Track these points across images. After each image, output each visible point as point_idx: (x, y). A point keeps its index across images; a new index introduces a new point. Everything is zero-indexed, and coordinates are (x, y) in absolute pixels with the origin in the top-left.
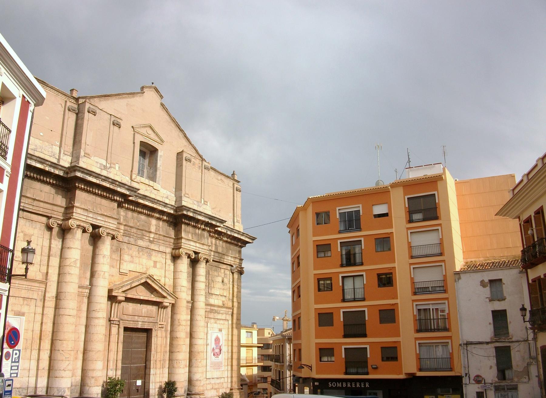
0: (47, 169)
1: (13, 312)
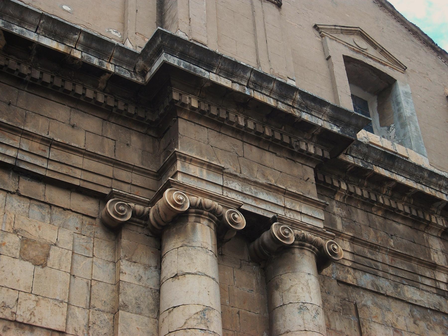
0: (77, 54)
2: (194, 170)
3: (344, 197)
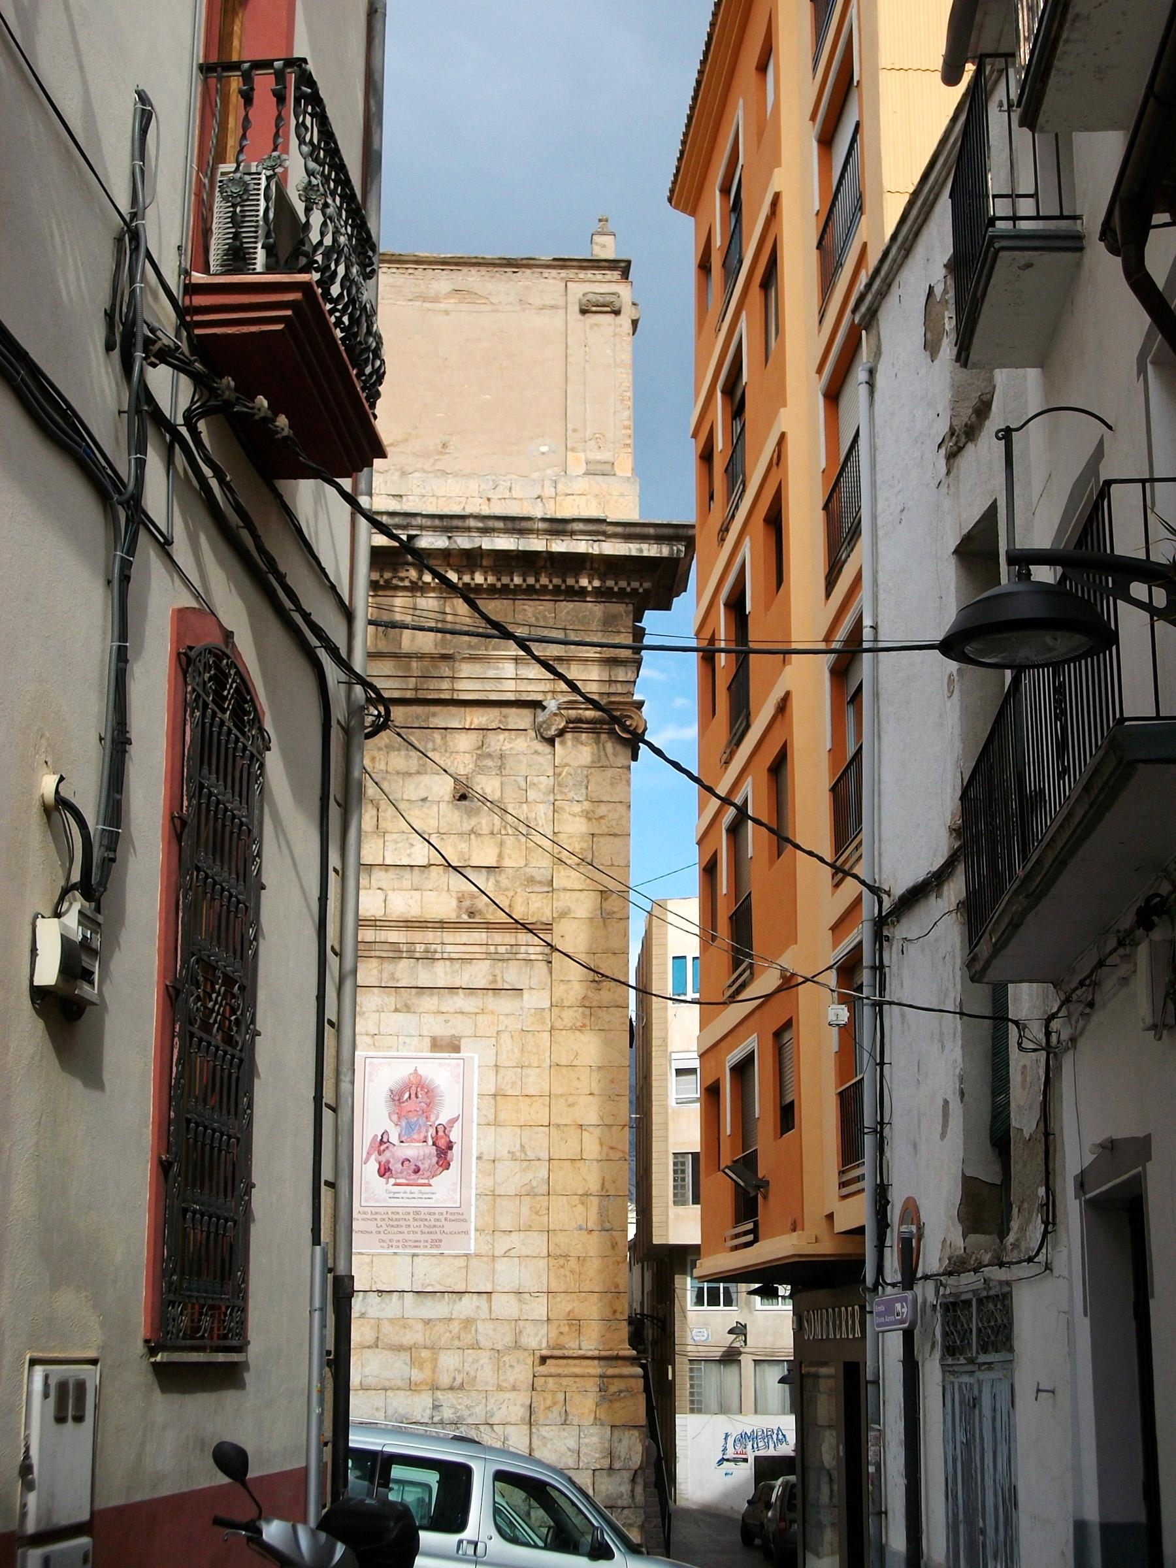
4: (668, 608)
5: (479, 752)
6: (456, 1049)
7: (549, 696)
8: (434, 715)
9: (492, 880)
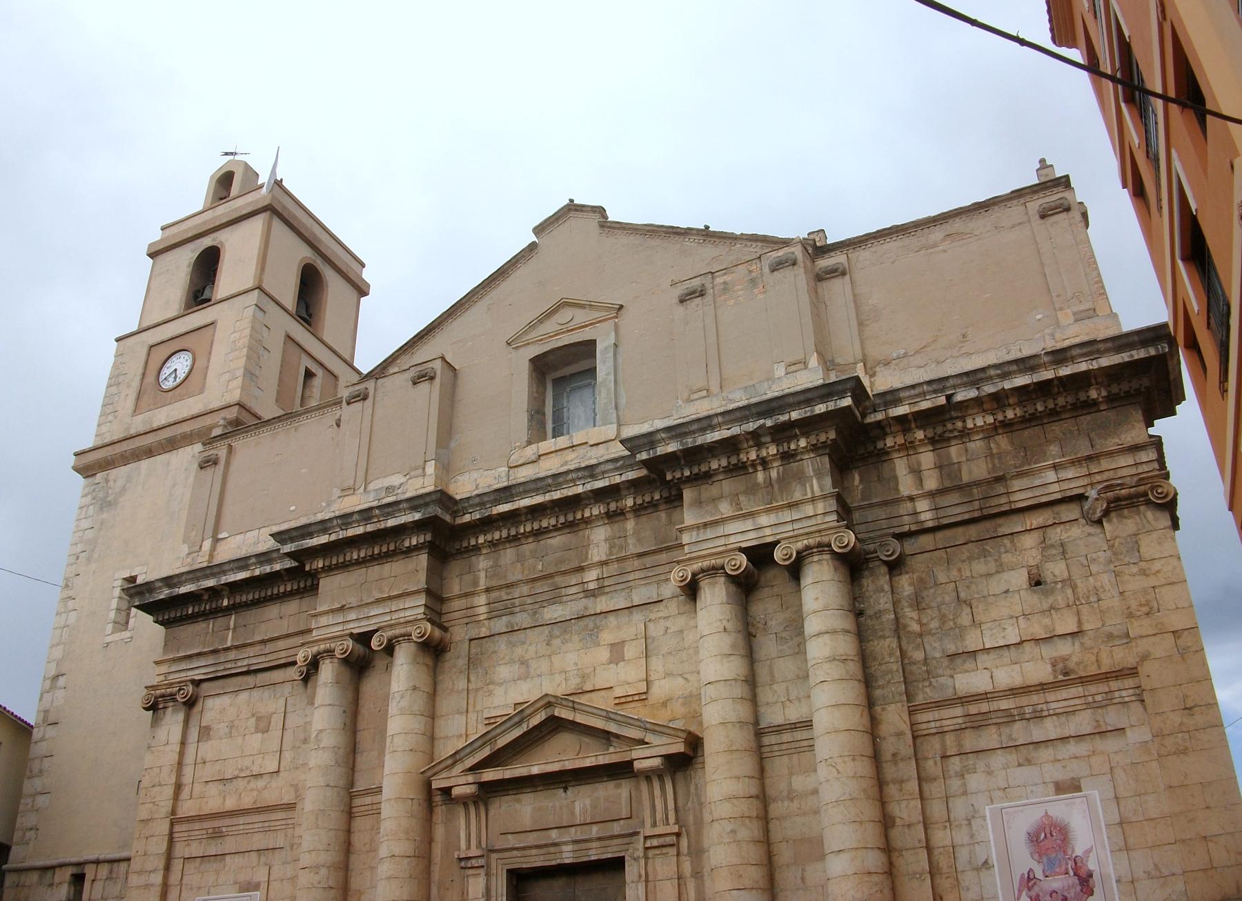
0: (257, 572)
1: (238, 885)
2: (324, 620)
3: (490, 547)
4: (1174, 413)
5: (1044, 545)
6: (1078, 788)
7: (1089, 488)
8: (1000, 526)
9: (1077, 644)
